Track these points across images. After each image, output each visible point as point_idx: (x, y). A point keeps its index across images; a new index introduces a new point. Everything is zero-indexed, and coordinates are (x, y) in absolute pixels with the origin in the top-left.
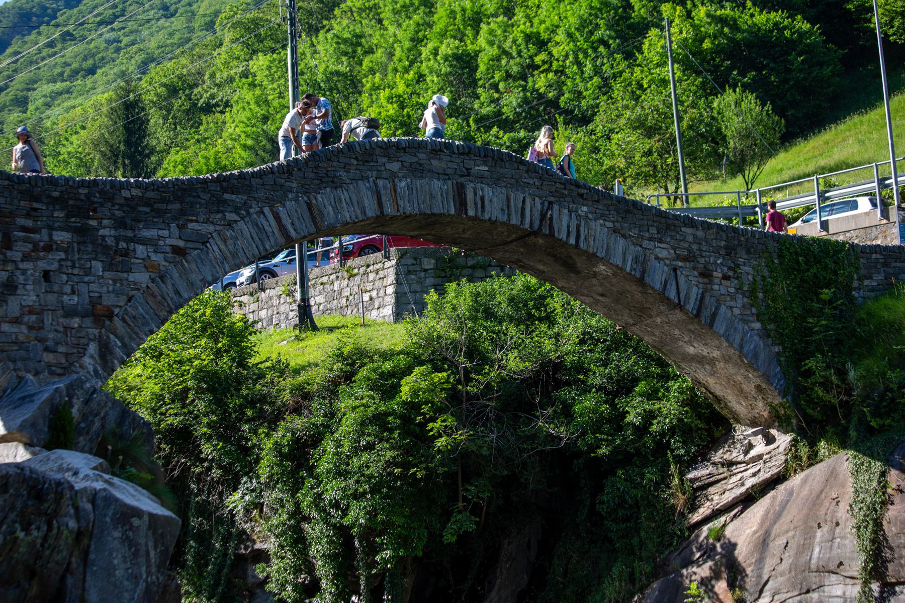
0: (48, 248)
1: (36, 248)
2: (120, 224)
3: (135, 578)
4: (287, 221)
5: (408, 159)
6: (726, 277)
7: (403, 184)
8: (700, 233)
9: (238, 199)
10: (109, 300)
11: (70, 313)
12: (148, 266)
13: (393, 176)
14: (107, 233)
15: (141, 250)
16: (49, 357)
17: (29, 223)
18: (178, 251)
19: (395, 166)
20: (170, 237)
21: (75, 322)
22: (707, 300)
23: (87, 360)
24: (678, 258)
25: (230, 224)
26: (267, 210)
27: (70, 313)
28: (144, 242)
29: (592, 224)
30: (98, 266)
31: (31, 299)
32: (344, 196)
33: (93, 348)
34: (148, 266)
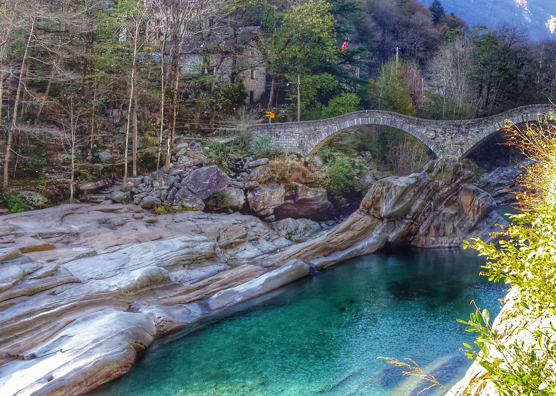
1: (450, 133)
2: (466, 128)
3: (395, 194)
5: (531, 109)
7: (529, 115)
9: (491, 121)
12: (471, 135)
13: (527, 114)
14: (464, 130)
15: (470, 132)
16: (451, 152)
17: (449, 129)
18: (478, 132)
19: (527, 111)
20: (476, 129)
21: (457, 145)
23: (458, 152)
25: (489, 126)
26: (497, 123)
30: (461, 136)
31: (448, 142)
32: (515, 119)
34: (473, 135)
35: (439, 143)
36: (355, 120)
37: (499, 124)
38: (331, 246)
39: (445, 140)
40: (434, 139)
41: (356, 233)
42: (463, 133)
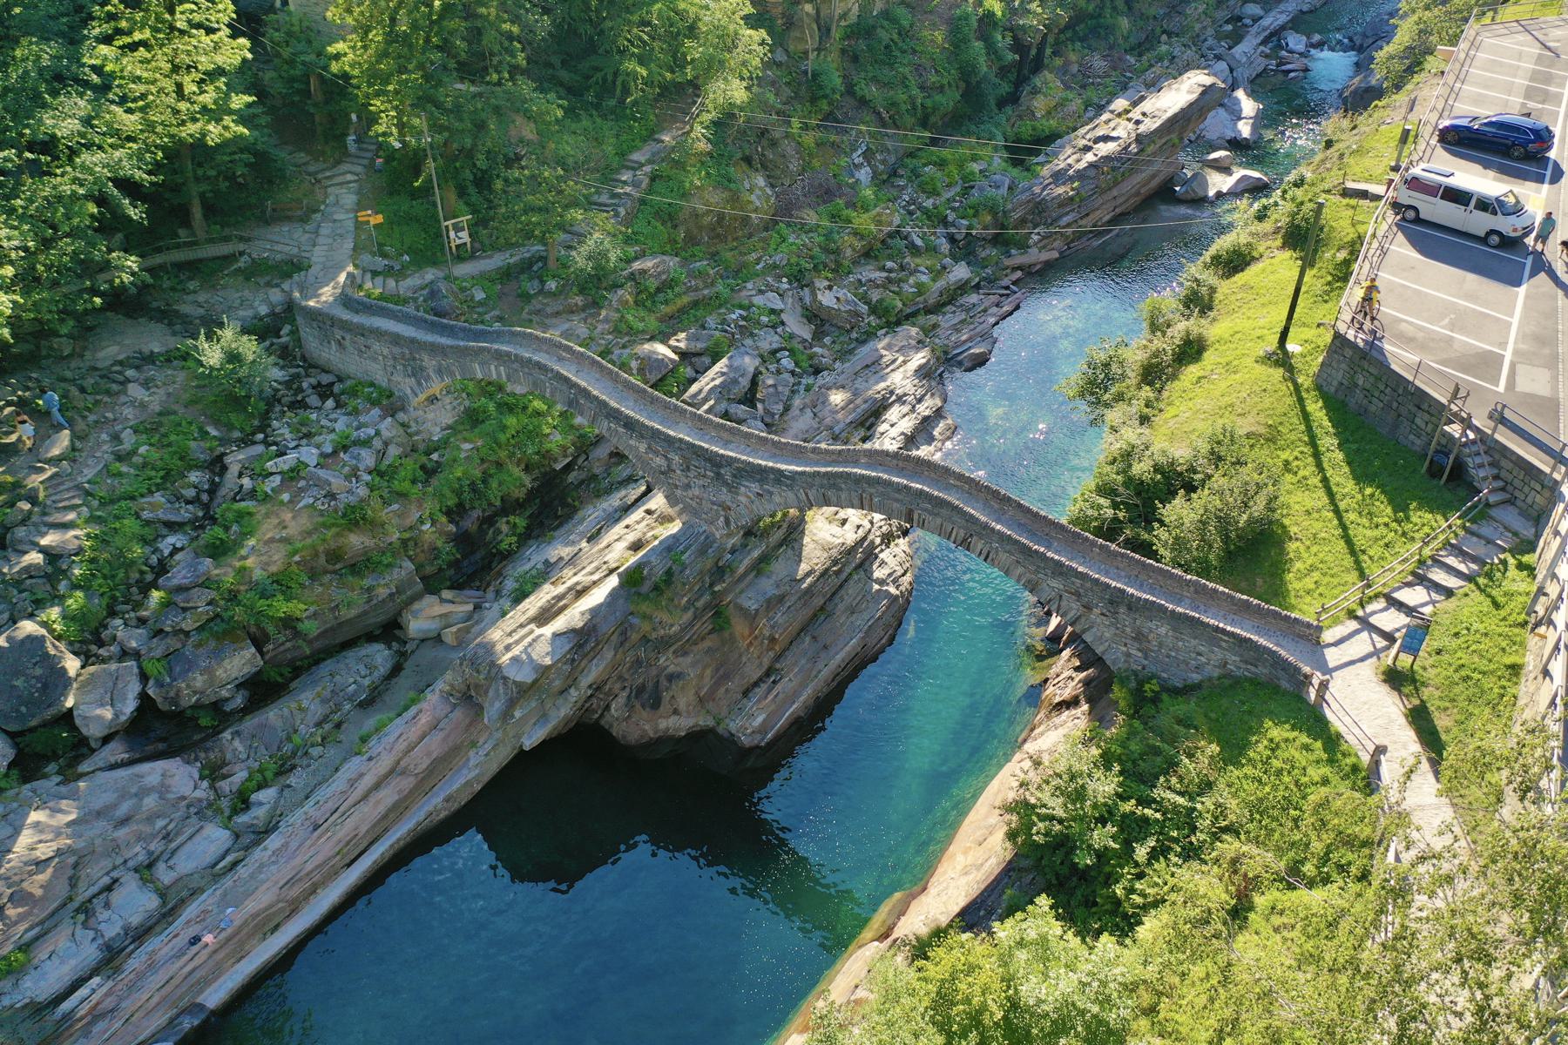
0: (704, 476)
4: (811, 498)
6: (1103, 614)
8: (1088, 585)
10: (729, 504)
11: (713, 503)
14: (728, 478)
15: (743, 489)
20: (755, 487)
22: (1083, 620)
24: (1066, 591)
27: (713, 503)
28: (746, 487)
29: (1001, 554)
30: (724, 490)
31: (697, 493)
33: (722, 519)
35: (676, 487)
36: (493, 367)
37: (806, 494)
38: (295, 892)
39: (688, 486)
40: (663, 473)
41: (407, 783)
42: (726, 484)
